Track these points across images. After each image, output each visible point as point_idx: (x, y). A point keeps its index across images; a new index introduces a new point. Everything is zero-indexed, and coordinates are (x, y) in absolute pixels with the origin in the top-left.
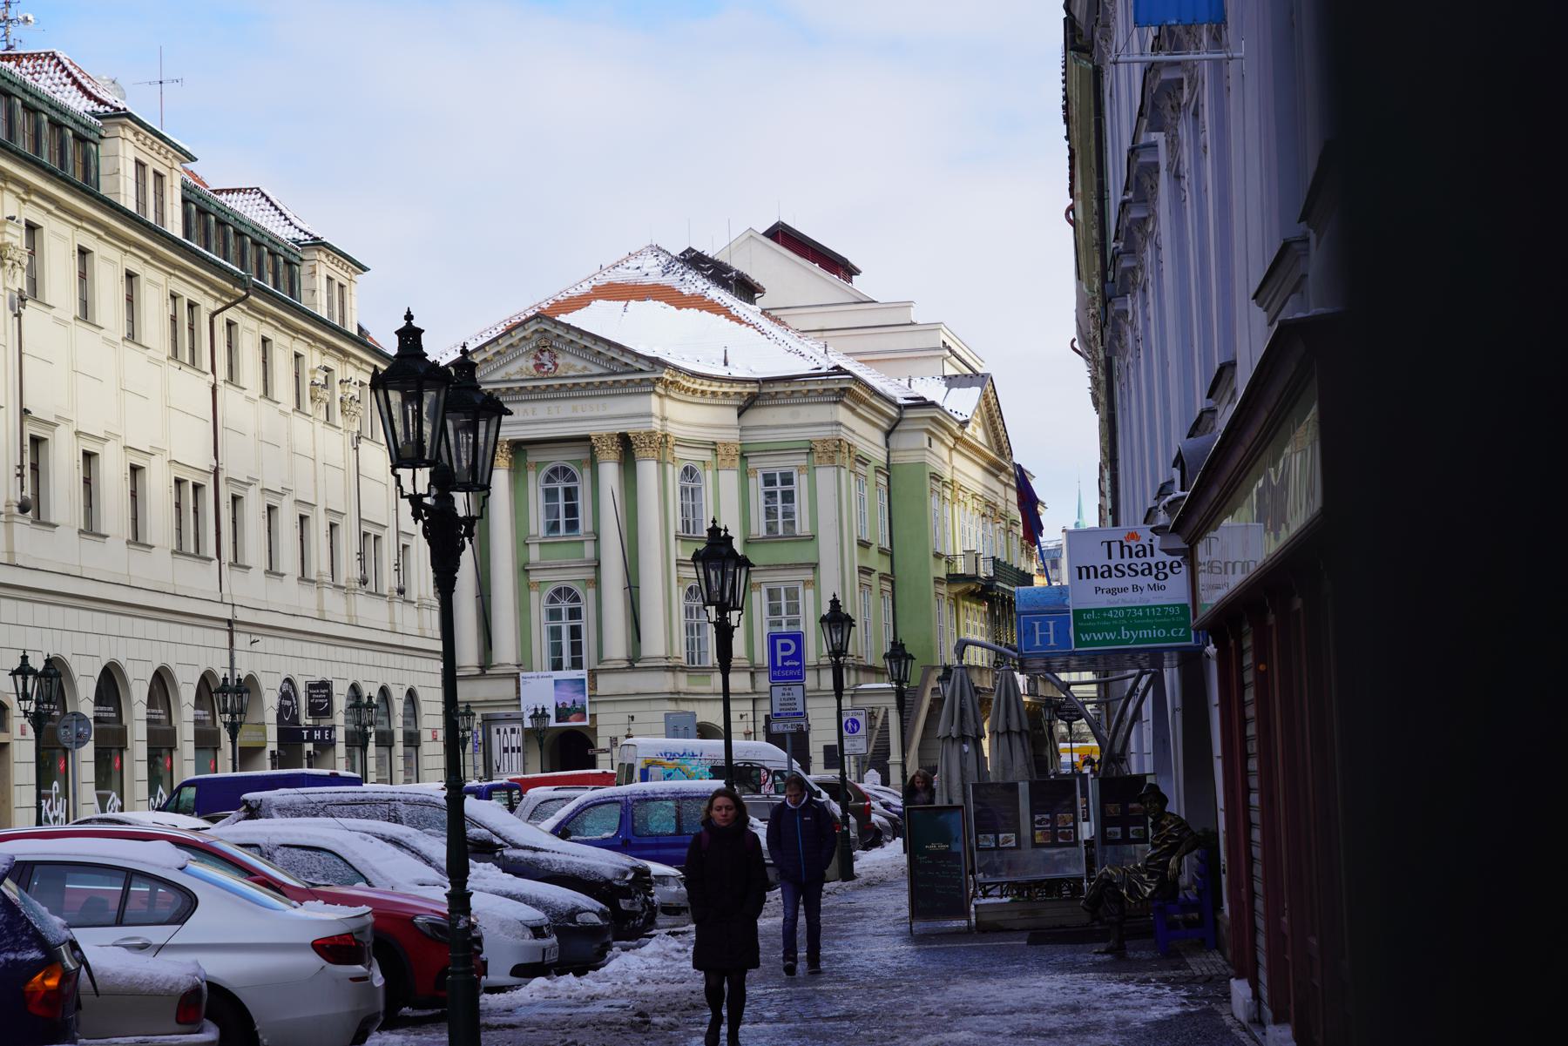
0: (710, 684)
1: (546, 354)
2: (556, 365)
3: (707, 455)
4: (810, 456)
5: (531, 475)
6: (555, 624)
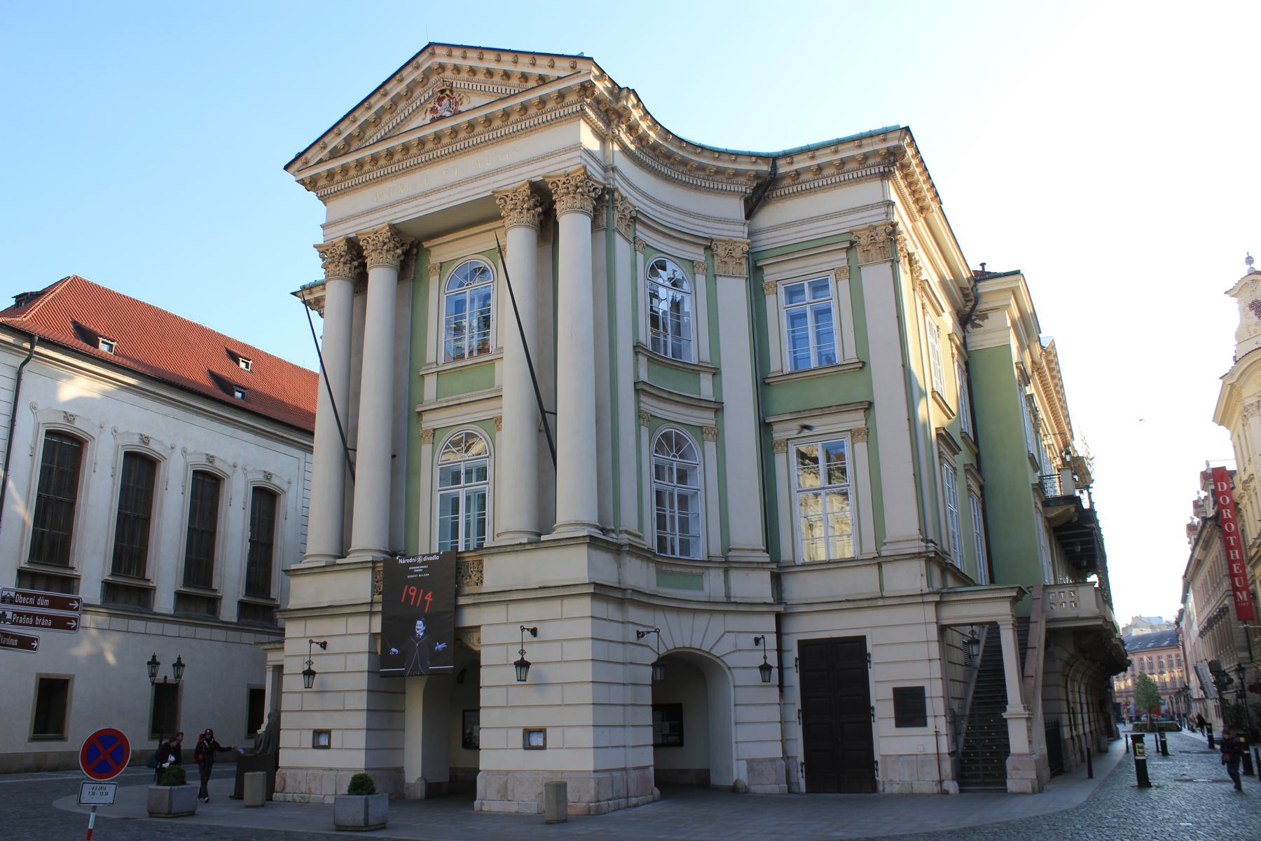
1: (445, 102)
3: (698, 255)
4: (852, 253)
5: (434, 281)
6: (451, 490)
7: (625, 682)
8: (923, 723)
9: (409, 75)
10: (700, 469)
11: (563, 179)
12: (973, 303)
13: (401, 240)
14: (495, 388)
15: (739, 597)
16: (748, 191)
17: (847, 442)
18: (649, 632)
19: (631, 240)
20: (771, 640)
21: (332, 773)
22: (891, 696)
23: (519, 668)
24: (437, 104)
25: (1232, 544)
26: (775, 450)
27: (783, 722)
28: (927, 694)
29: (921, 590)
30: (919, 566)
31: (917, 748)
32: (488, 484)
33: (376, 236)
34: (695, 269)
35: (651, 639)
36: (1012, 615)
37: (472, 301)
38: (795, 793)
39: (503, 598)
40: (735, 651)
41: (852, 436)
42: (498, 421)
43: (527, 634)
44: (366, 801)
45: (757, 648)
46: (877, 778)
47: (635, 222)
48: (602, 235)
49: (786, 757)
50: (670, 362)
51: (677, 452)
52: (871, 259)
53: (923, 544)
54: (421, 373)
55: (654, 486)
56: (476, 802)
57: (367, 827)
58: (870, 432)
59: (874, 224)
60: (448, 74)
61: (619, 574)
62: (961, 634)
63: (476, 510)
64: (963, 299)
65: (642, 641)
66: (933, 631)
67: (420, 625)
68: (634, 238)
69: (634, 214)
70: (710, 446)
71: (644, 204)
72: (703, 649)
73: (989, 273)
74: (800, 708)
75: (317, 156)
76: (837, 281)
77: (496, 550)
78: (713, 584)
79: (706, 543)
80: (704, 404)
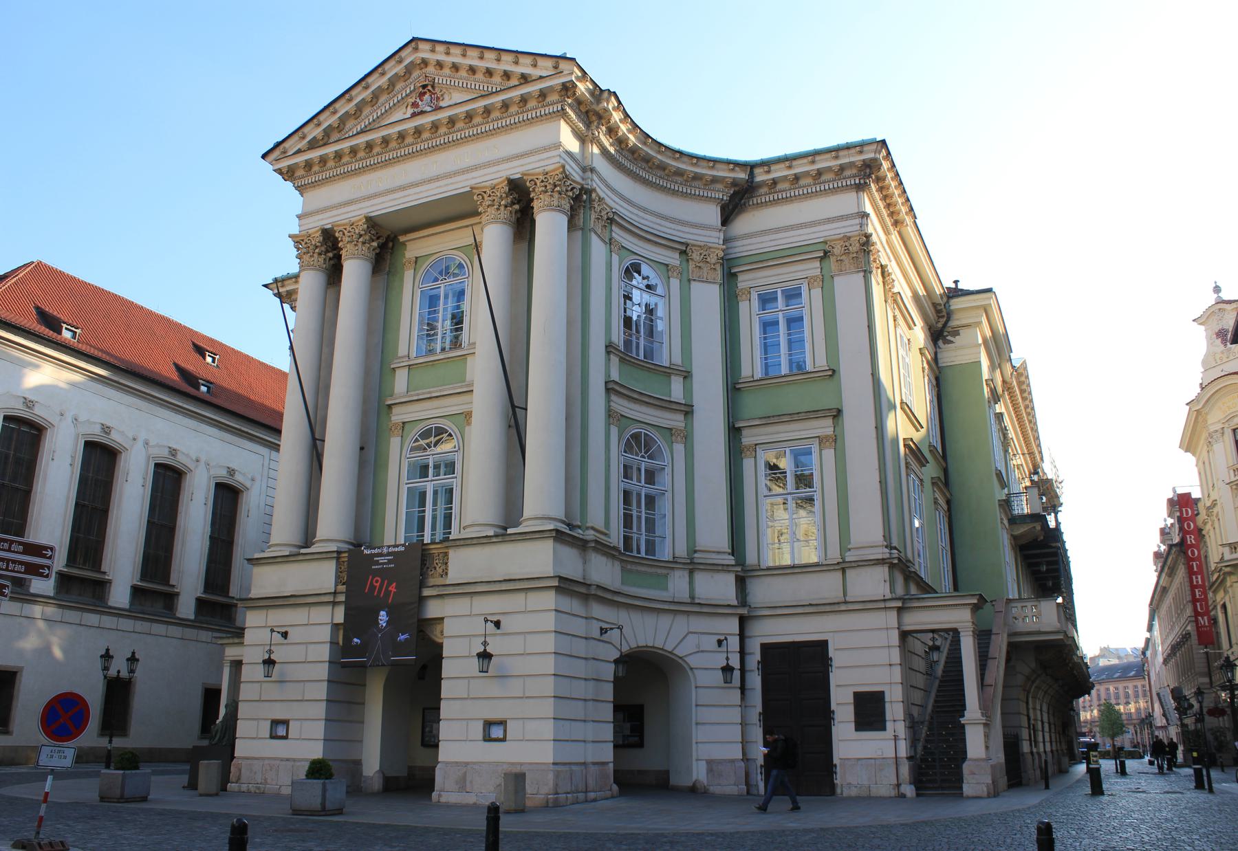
0: (666, 589)
1: (427, 97)
3: (673, 259)
4: (826, 263)
5: (408, 275)
6: (419, 483)
7: (587, 677)
8: (884, 729)
9: (391, 69)
10: (668, 470)
11: (541, 177)
12: (945, 319)
13: (377, 233)
14: (466, 383)
15: (703, 599)
16: (725, 198)
17: (815, 448)
18: (612, 629)
19: (607, 241)
20: (734, 643)
21: (288, 763)
22: (852, 701)
23: (481, 660)
24: (418, 99)
25: (1195, 569)
26: (743, 455)
27: (744, 724)
28: (887, 698)
29: (884, 596)
30: (882, 572)
31: (876, 752)
32: (456, 478)
33: (352, 228)
34: (670, 273)
35: (614, 635)
36: (973, 623)
37: (446, 297)
38: (755, 795)
39: (468, 590)
40: (698, 652)
41: (820, 443)
42: (468, 415)
43: (490, 626)
44: (324, 785)
45: (720, 649)
46: (835, 781)
47: (611, 224)
48: (579, 233)
49: (746, 759)
50: (641, 363)
51: (646, 453)
52: (843, 269)
53: (887, 550)
54: (392, 366)
55: (622, 485)
56: (434, 794)
57: (324, 811)
58: (838, 441)
59: (848, 234)
60: (431, 69)
61: (584, 570)
62: (922, 642)
63: (443, 503)
64: (935, 316)
65: (605, 637)
66: (895, 637)
67: (383, 615)
68: (610, 239)
69: (611, 215)
70: (679, 448)
71: (621, 206)
72: (665, 648)
73: (962, 290)
74: (761, 711)
75: (295, 147)
76: (810, 290)
77: (462, 543)
78: (678, 584)
79: (672, 544)
80: (674, 406)
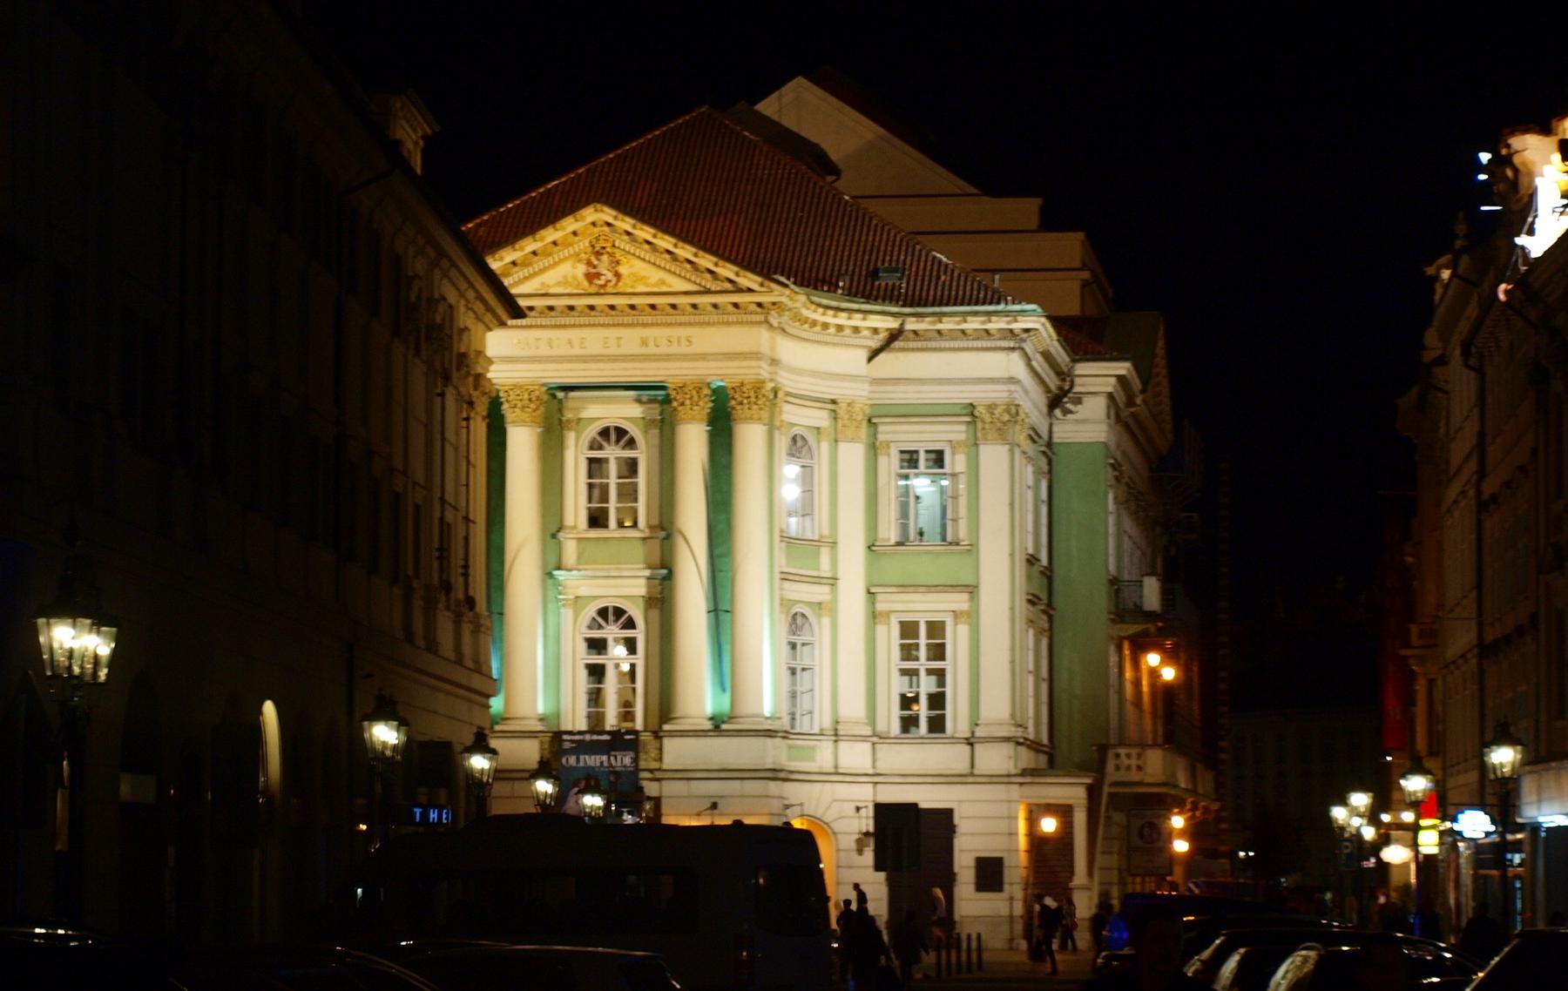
0: (813, 759)
1: (605, 258)
2: (618, 275)
3: (821, 418)
22: (972, 863)
30: (1007, 749)
53: (1013, 729)
70: (826, 621)
